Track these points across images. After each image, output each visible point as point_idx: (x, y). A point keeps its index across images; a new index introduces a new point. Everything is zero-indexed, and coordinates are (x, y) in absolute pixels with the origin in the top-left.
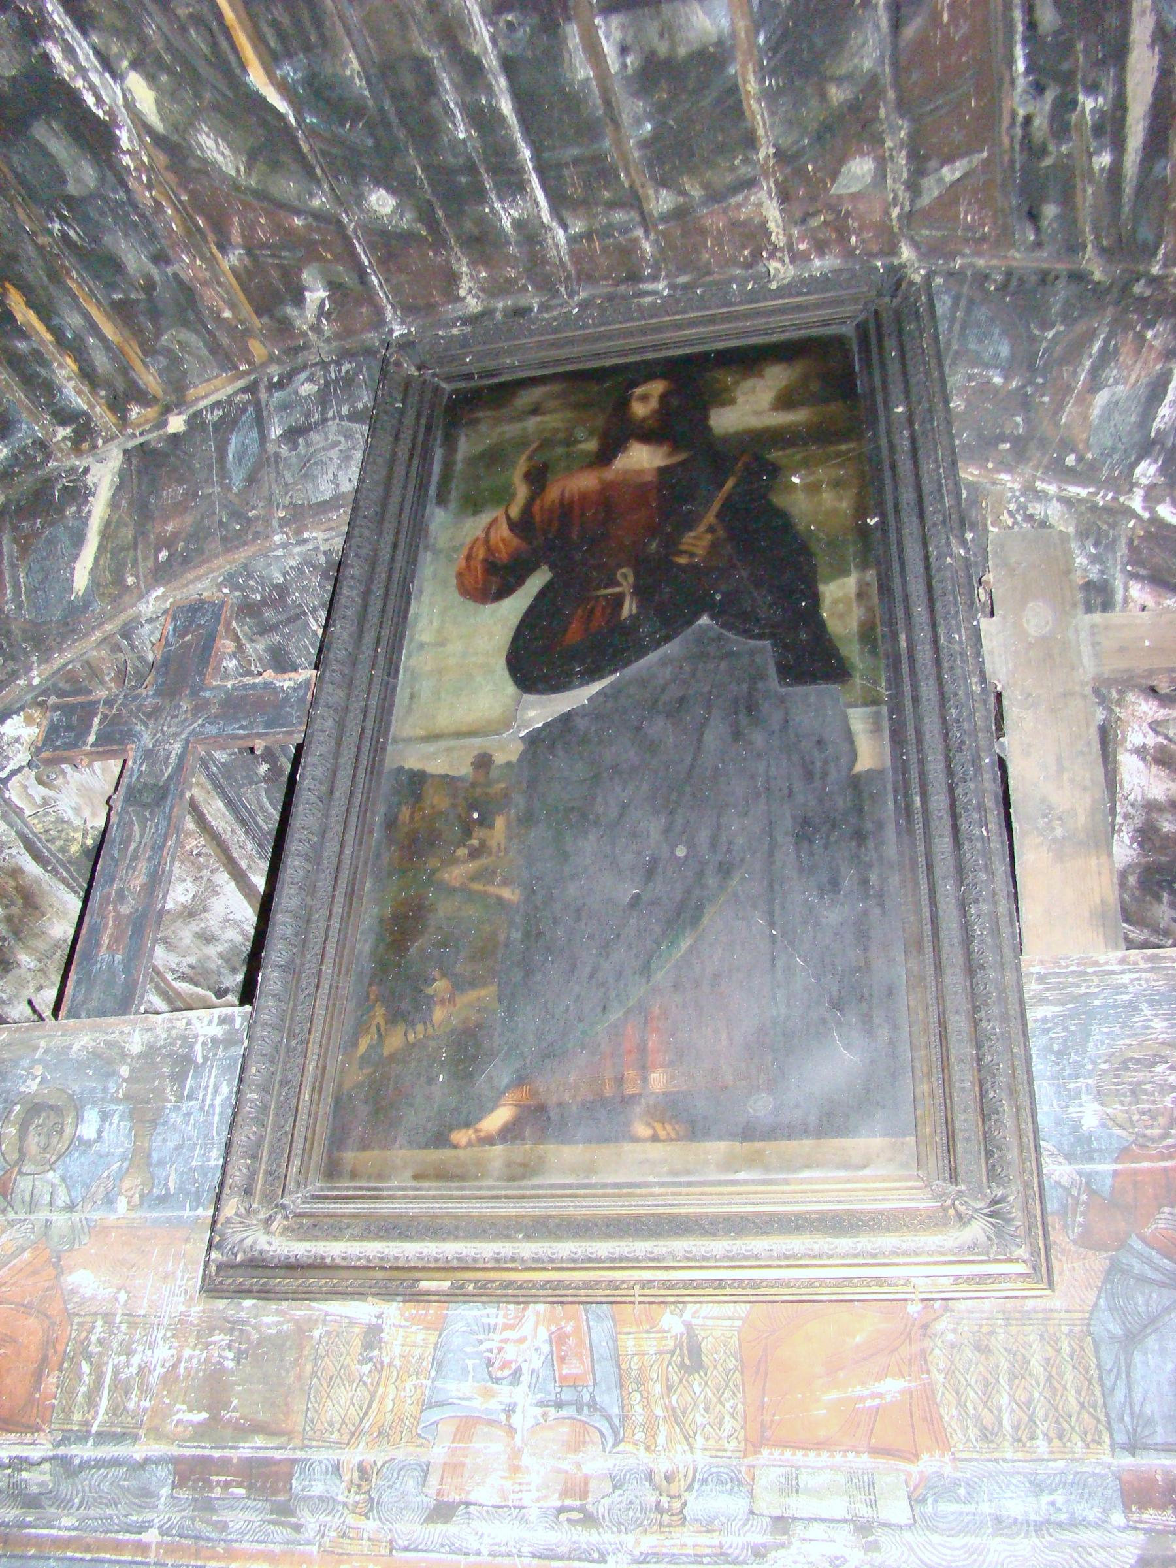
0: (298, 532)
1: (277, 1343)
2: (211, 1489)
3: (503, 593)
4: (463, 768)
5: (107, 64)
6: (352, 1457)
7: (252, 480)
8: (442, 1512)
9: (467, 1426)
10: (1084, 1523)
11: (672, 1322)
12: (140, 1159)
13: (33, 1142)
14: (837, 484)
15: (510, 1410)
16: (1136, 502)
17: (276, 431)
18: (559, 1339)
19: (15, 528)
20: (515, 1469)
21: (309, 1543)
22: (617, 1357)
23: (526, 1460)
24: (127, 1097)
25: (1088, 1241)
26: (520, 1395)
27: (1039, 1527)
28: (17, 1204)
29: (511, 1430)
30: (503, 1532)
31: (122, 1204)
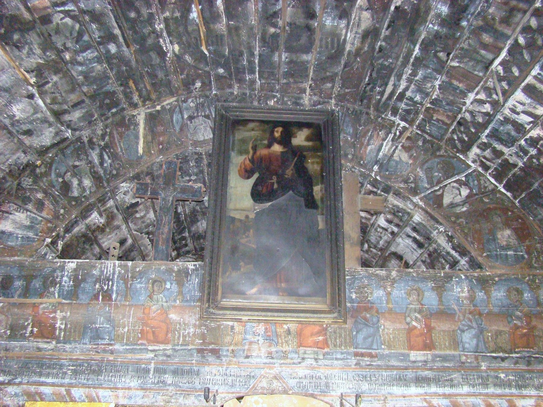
0: (195, 148)
1: (214, 329)
3: (248, 178)
4: (243, 218)
5: (171, 42)
6: (231, 348)
7: (181, 129)
8: (247, 357)
9: (251, 343)
10: (348, 359)
11: (285, 327)
12: (180, 293)
13: (156, 288)
14: (317, 163)
15: (258, 340)
16: (373, 175)
17: (186, 116)
18: (266, 329)
19: (117, 130)
20: (260, 350)
22: (276, 332)
23: (261, 349)
24: (176, 280)
25: (352, 317)
26: (260, 338)
27: (342, 359)
28: (154, 300)
29: (259, 344)
30: (258, 360)
31: (178, 301)
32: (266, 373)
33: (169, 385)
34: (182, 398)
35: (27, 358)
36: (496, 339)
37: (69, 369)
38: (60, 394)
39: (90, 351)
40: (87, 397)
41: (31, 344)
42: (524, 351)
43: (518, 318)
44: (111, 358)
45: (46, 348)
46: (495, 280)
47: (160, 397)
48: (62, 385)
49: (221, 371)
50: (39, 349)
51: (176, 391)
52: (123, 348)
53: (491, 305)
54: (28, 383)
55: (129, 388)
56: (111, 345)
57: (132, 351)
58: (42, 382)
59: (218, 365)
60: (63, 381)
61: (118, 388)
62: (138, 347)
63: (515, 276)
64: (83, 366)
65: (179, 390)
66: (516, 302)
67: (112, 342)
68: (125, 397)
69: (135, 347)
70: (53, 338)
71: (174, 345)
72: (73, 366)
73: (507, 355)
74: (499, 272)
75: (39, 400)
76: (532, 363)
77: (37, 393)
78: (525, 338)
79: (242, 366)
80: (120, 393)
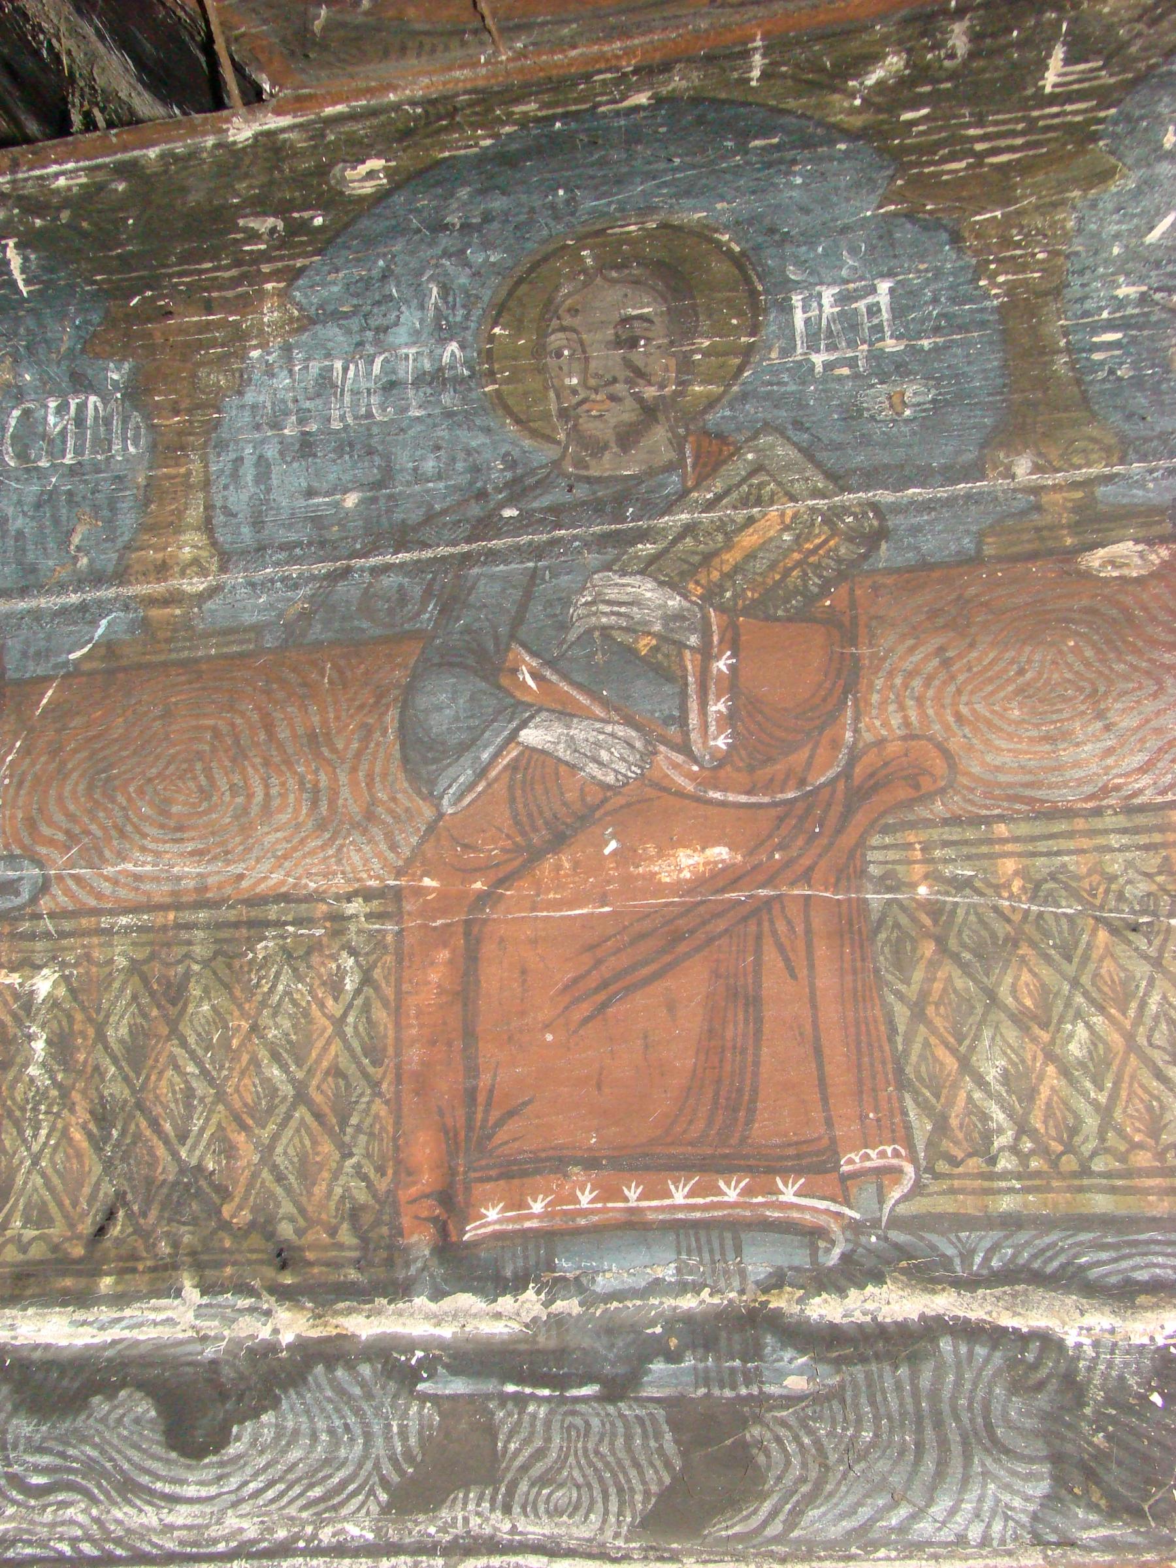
36: (136, 1054)
42: (635, 1229)
43: (620, 671)
46: (334, 200)
53: (189, 545)
63: (677, 82)
66: (628, 438)
73: (290, 1326)
74: (411, 84)
76: (783, 1452)
78: (692, 983)
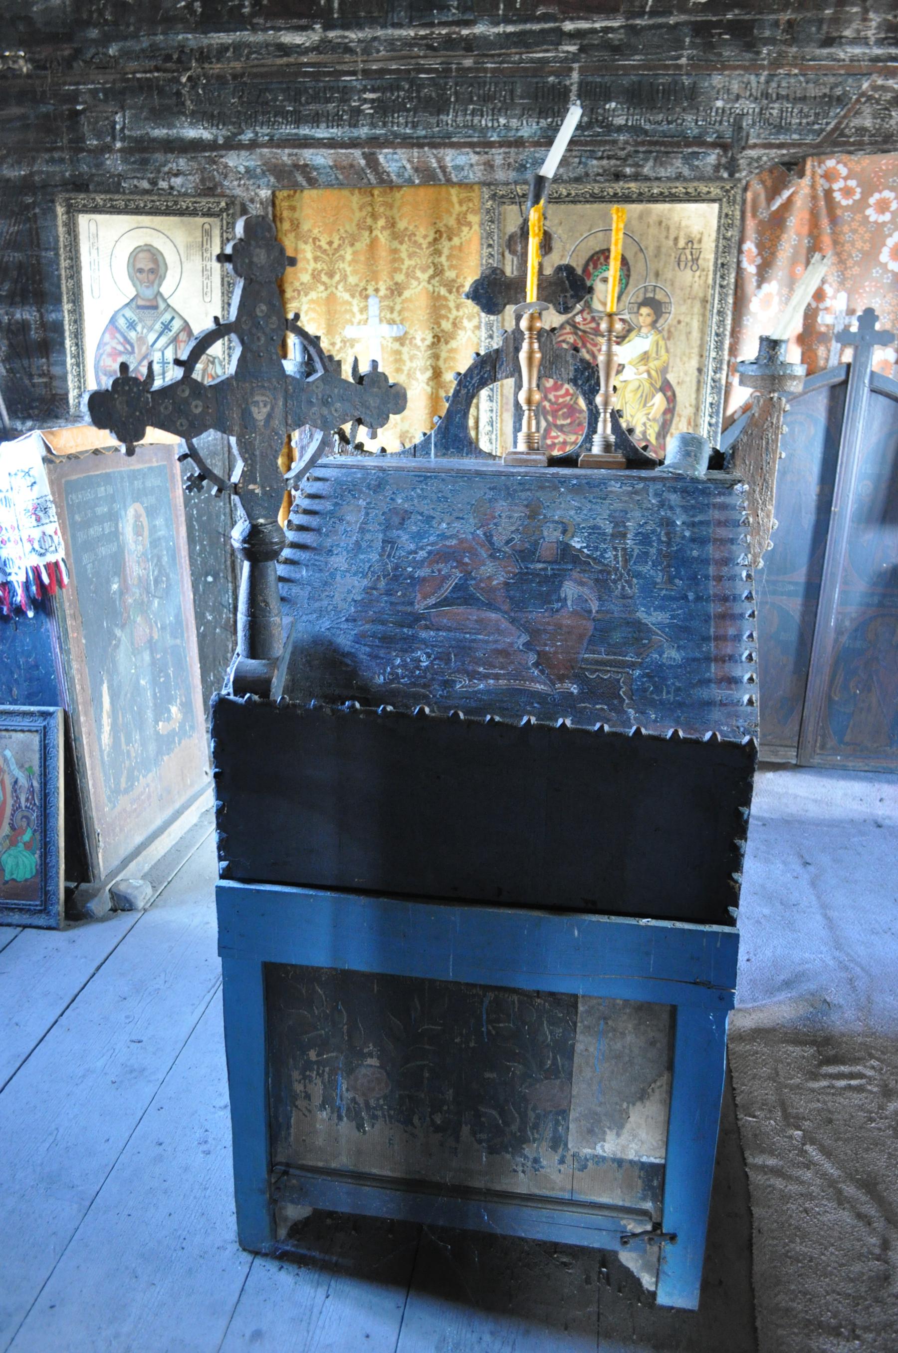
2: (713, 37)
8: (829, 42)
21: (763, 59)
30: (857, 51)
32: (875, 88)
33: (619, 129)
34: (651, 163)
35: (256, 75)
37: (365, 101)
38: (352, 166)
39: (411, 45)
40: (416, 170)
41: (260, 37)
44: (468, 62)
45: (299, 46)
47: (595, 162)
48: (354, 144)
49: (754, 85)
50: (284, 50)
51: (637, 144)
52: (495, 30)
54: (272, 143)
55: (519, 143)
56: (467, 23)
57: (521, 40)
58: (306, 138)
59: (745, 69)
60: (356, 132)
61: (491, 145)
62: (536, 27)
64: (399, 88)
65: (643, 143)
67: (469, 16)
68: (509, 164)
69: (528, 26)
70: (313, 17)
71: (631, 14)
72: (373, 90)
75: (304, 183)
77: (296, 166)
79: (812, 68)
80: (498, 156)
